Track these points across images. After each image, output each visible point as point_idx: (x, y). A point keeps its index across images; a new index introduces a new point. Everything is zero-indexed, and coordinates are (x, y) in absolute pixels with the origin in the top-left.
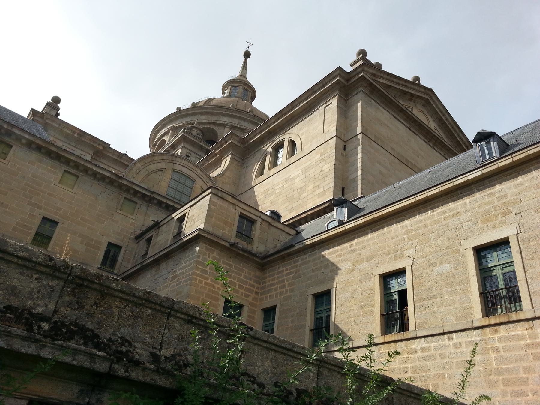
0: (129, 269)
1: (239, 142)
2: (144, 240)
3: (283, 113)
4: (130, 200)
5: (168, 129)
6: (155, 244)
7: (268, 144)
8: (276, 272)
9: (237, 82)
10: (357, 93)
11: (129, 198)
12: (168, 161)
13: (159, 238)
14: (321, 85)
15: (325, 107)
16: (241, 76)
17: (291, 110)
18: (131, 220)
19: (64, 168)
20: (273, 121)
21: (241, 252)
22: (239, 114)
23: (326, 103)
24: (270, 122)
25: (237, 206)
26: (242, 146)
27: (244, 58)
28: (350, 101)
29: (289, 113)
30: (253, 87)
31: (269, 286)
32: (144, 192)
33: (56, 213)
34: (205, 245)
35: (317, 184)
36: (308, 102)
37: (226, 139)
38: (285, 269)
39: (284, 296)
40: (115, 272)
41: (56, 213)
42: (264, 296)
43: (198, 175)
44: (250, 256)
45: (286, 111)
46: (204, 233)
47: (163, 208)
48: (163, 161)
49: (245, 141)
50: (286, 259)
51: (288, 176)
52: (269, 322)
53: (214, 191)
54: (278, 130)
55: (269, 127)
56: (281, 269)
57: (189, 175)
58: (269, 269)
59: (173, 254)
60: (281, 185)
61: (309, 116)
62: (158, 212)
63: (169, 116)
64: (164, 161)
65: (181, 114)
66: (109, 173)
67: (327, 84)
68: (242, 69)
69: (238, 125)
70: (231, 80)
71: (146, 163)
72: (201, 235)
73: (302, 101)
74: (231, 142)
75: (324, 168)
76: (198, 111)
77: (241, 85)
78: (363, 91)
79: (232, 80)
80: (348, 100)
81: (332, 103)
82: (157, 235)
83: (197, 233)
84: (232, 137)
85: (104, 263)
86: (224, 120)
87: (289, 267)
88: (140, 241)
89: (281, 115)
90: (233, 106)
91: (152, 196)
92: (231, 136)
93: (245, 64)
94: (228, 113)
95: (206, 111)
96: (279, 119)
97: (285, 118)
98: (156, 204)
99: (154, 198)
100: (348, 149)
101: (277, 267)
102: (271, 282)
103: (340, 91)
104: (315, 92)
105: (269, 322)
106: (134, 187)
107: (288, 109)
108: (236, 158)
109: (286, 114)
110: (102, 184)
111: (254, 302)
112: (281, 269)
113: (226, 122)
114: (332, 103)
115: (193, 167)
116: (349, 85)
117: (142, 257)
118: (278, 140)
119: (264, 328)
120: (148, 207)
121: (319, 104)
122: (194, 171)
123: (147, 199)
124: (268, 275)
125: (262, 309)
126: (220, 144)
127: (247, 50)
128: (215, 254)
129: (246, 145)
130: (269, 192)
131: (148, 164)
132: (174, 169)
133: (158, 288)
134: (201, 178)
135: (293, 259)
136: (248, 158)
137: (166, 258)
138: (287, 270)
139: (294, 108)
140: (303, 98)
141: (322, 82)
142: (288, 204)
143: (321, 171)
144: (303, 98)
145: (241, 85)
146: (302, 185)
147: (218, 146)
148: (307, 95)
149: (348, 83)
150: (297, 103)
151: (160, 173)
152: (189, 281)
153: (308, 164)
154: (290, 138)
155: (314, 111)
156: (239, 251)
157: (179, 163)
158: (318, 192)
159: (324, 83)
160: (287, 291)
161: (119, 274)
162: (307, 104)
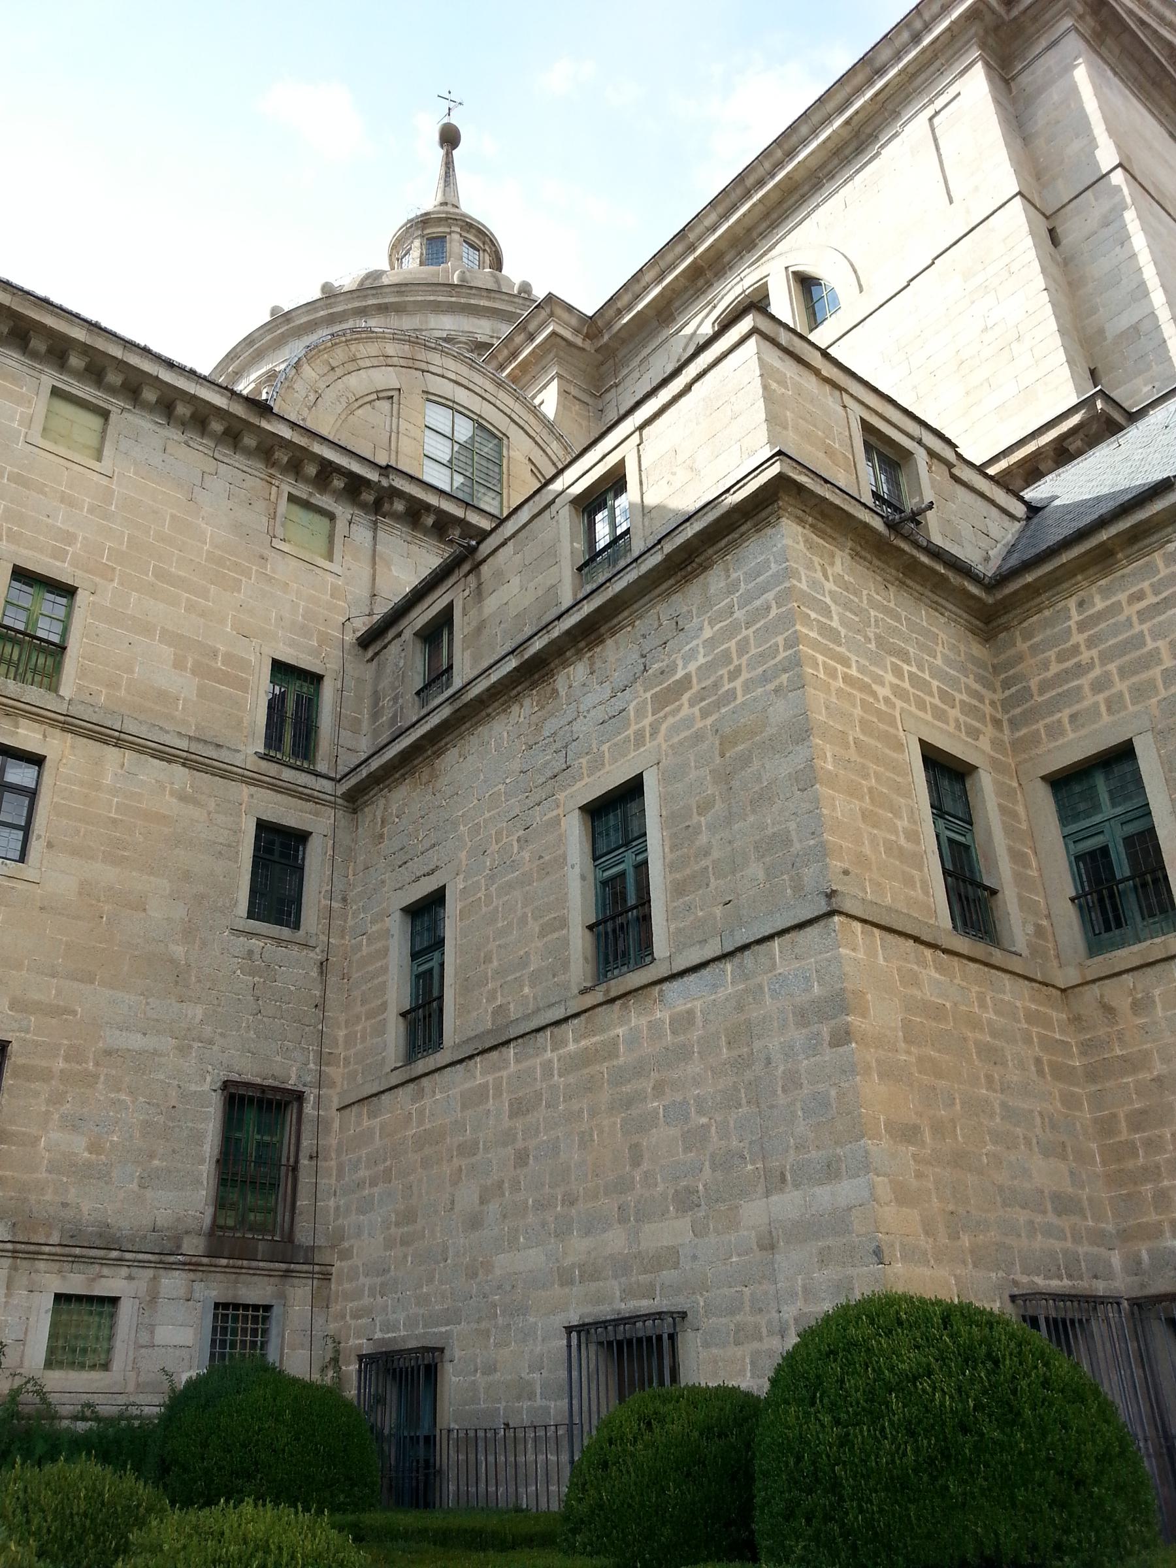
0: (364, 756)
1: (577, 331)
2: (408, 634)
3: (750, 182)
4: (306, 505)
5: (253, 385)
6: (480, 628)
7: (696, 314)
8: (1072, 623)
9: (440, 221)
10: (1054, 43)
11: (305, 496)
12: (403, 362)
13: (491, 604)
14: (905, 36)
15: (931, 119)
16: (444, 204)
17: (779, 165)
18: (330, 578)
19: (50, 378)
20: (708, 222)
21: (924, 559)
22: (489, 298)
23: (931, 101)
24: (699, 230)
25: (846, 391)
26: (587, 345)
27: (441, 152)
28: (1025, 79)
29: (773, 176)
30: (491, 233)
31: (1044, 687)
32: (356, 467)
33: (59, 555)
34: (800, 529)
36: (851, 118)
37: (531, 327)
38: (1122, 597)
39: (1163, 693)
40: (322, 767)
41: (59, 555)
42: (1040, 725)
43: (509, 417)
44: (950, 575)
45: (761, 171)
46: (800, 473)
47: (426, 532)
48: (386, 361)
49: (600, 323)
50: (1120, 556)
52: (1098, 818)
53: (765, 325)
54: (727, 259)
55: (695, 249)
56: (1100, 604)
57: (479, 416)
58: (1025, 624)
59: (626, 613)
61: (858, 171)
62: (412, 547)
63: (249, 340)
64: (389, 361)
65: (292, 325)
66: (222, 395)
67: (927, 27)
68: (442, 185)
69: (492, 337)
70: (417, 217)
71: (333, 369)
72: (789, 477)
73: (827, 120)
74: (554, 334)
76: (350, 306)
77: (453, 229)
78: (1076, 29)
79: (422, 215)
80: (1013, 78)
81: (959, 94)
82: (479, 594)
83: (775, 470)
84: (551, 315)
85: (273, 737)
87: (1146, 585)
88: (385, 647)
89: (739, 191)
90: (462, 278)
91: (385, 483)
92: (548, 310)
93: (449, 164)
94: (453, 299)
95: (375, 301)
96: (734, 208)
97: (760, 201)
98: (396, 517)
99: (396, 493)
100: (1066, 241)
101: (1072, 603)
102: (1055, 668)
103: (983, 46)
104: (880, 71)
105: (1098, 818)
106: (318, 449)
107: (767, 165)
108: (574, 391)
109: (761, 183)
110: (201, 444)
111: (1001, 757)
112: (1100, 604)
113: (452, 333)
114: (959, 94)
115: (490, 387)
116: (1015, 19)
117: (416, 698)
118: (738, 290)
119: (1071, 846)
120: (375, 530)
121: (896, 115)
122: (492, 399)
123: (368, 497)
124: (1022, 646)
125: (1043, 778)
126: (506, 352)
127: (446, 120)
128: (838, 568)
129: (606, 338)
131: (339, 372)
132: (427, 392)
133: (584, 761)
134: (522, 428)
135: (1162, 547)
136: (616, 385)
137: (582, 644)
138: (1139, 596)
139: (790, 154)
140: (830, 106)
141: (908, 25)
143: (985, 330)
144: (830, 106)
145: (453, 229)
147: (501, 359)
148: (848, 89)
149: (1008, 11)
150: (804, 130)
151: (384, 405)
152: (785, 671)
154: (791, 269)
155: (882, 147)
156: (915, 552)
157: (439, 371)
159: (918, 25)
161: (338, 777)
162: (849, 128)
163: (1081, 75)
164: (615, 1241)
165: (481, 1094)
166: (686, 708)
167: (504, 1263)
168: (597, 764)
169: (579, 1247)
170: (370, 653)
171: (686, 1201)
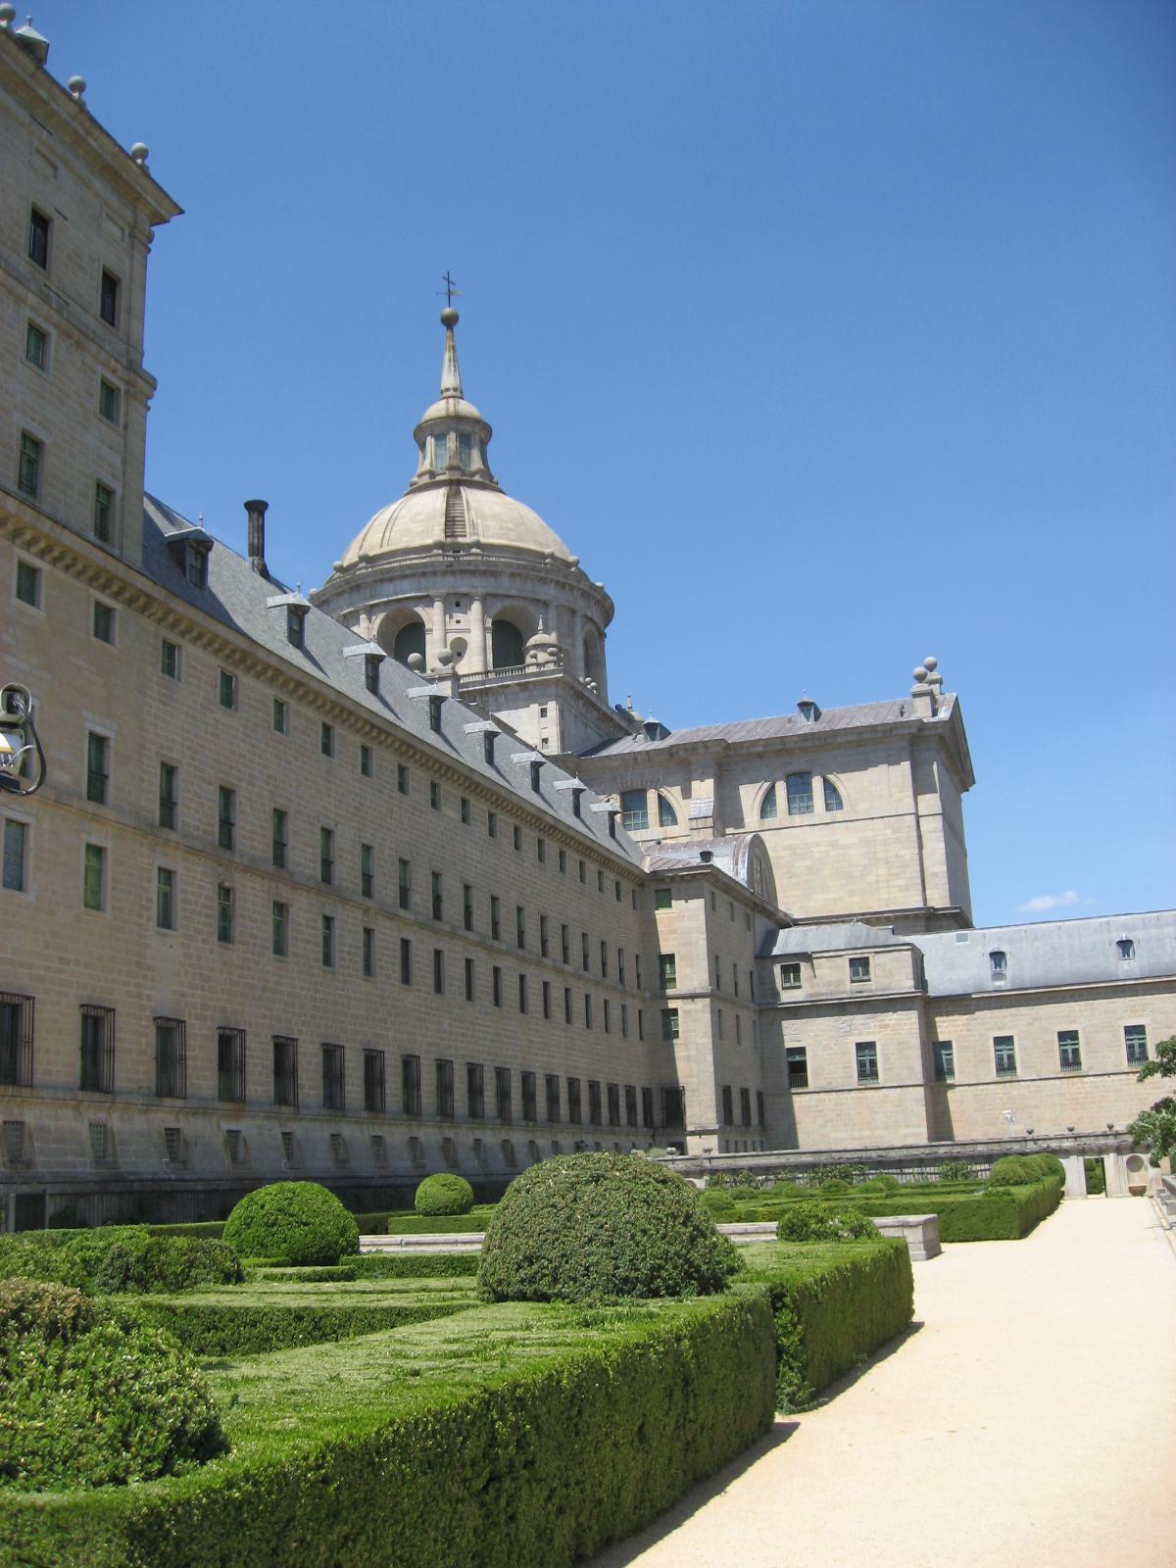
60: (823, 849)
75: (901, 853)
86: (548, 592)
130: (798, 851)
143: (897, 855)
153: (870, 834)
164: (867, 1133)
165: (825, 1100)
167: (834, 1135)
168: (860, 1034)
169: (857, 1134)
170: (758, 961)
171: (886, 1127)
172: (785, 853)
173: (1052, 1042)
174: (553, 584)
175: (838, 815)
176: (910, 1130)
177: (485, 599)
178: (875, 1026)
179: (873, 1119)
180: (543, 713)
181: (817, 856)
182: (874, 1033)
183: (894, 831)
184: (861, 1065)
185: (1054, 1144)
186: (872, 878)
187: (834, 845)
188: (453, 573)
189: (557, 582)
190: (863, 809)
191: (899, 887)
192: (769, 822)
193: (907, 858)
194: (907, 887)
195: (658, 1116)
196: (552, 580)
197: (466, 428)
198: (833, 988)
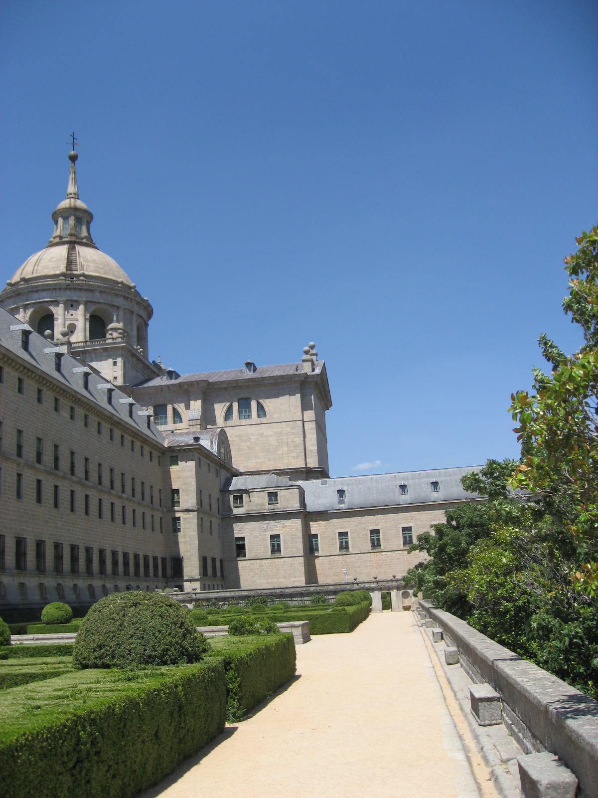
35: (290, 449)
51: (261, 432)
60: (256, 437)
86: (120, 301)
130: (243, 438)
142: (265, 453)
143: (292, 441)
146: (277, 444)
153: (280, 430)
158: (292, 454)
160: (323, 529)
163: (313, 397)
164: (275, 580)
165: (254, 563)
166: (286, 529)
167: (258, 581)
168: (273, 530)
169: (270, 581)
170: (222, 493)
171: (285, 577)
172: (237, 439)
173: (367, 535)
174: (122, 298)
175: (264, 420)
176: (296, 579)
177: (86, 304)
178: (280, 527)
179: (278, 573)
180: (115, 364)
181: (253, 440)
182: (279, 530)
183: (291, 429)
184: (273, 546)
185: (367, 585)
186: (280, 452)
187: (262, 435)
188: (70, 289)
189: (124, 297)
190: (276, 417)
191: (293, 456)
192: (229, 423)
193: (298, 442)
194: (297, 457)
195: (169, 572)
196: (121, 295)
197: (80, 214)
198: (259, 507)
